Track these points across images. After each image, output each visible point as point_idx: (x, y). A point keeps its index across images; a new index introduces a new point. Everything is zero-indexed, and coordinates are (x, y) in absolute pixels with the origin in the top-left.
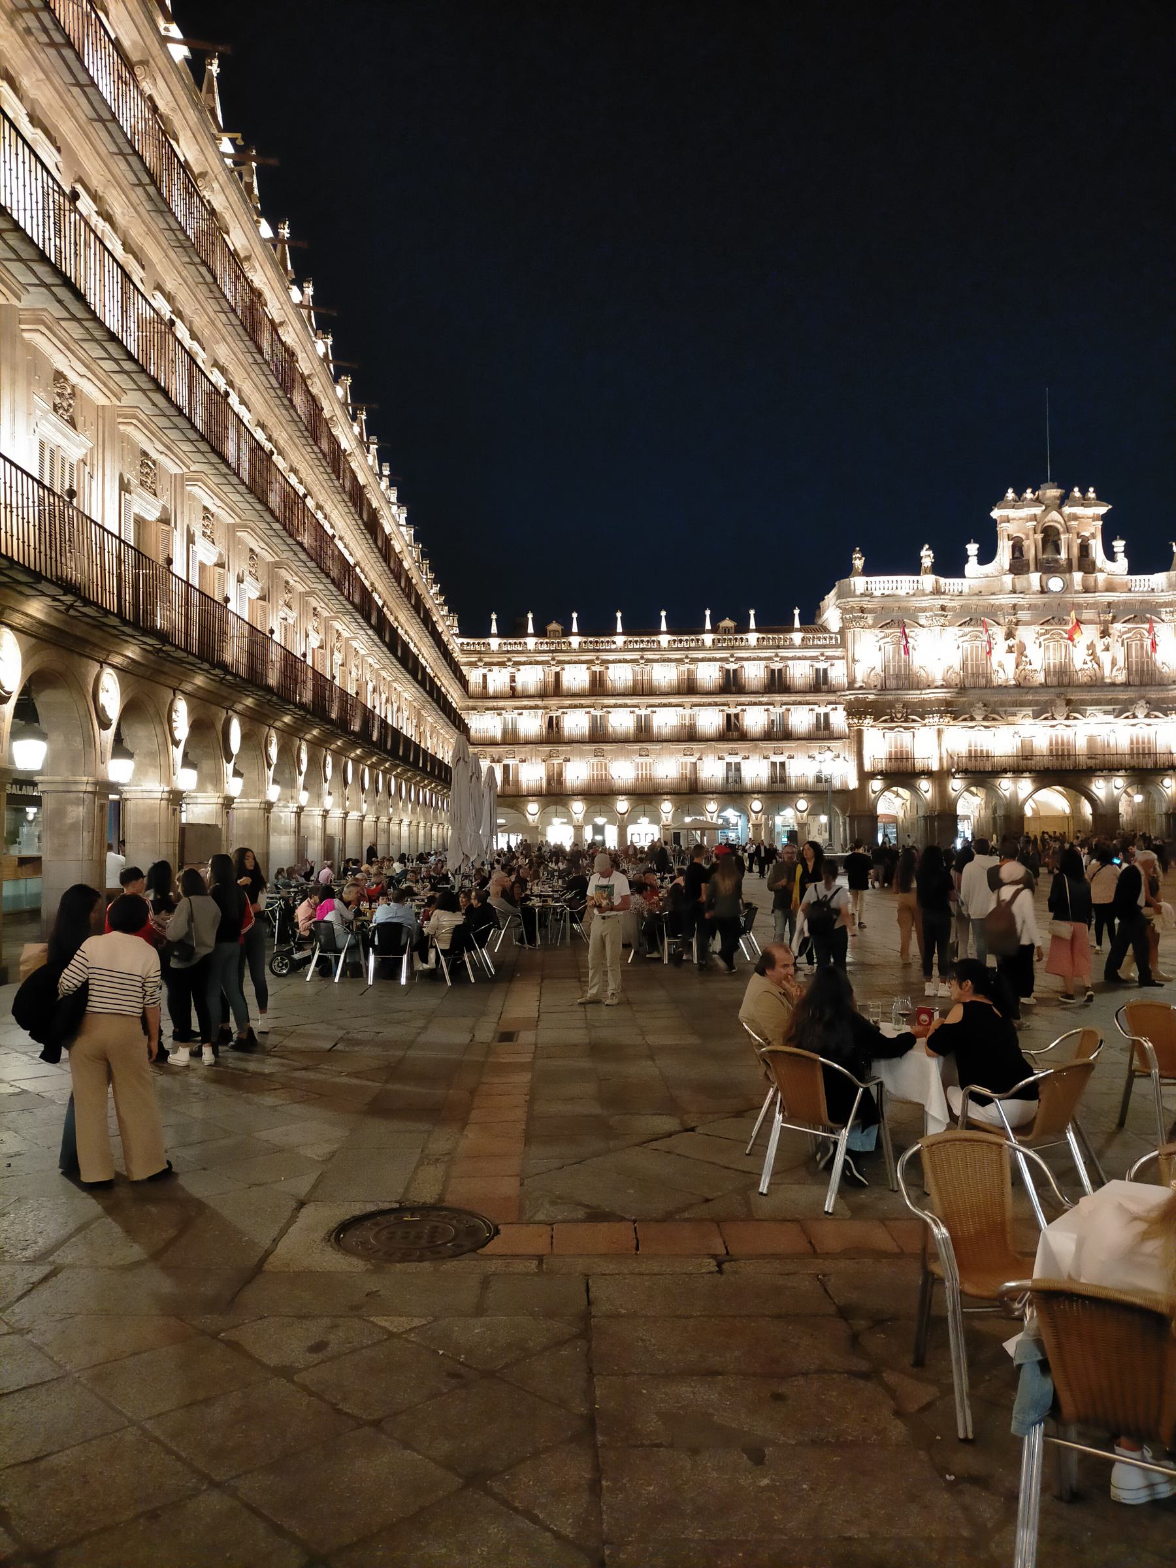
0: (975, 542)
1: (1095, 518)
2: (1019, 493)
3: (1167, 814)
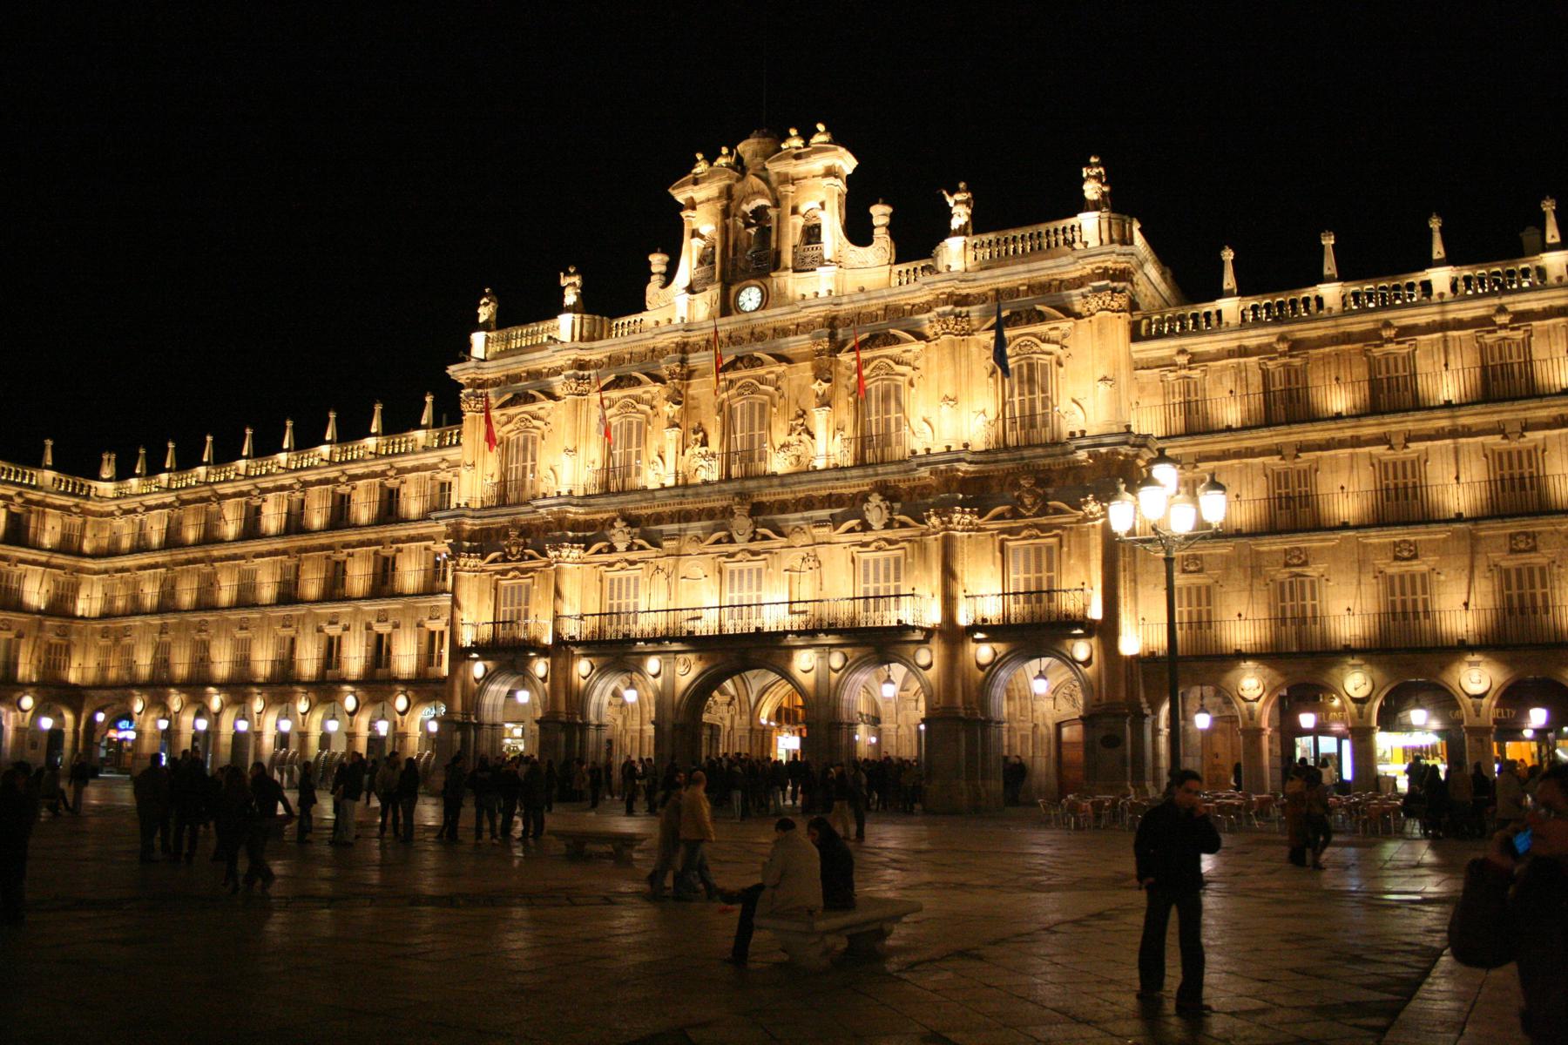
0: (663, 252)
1: (830, 172)
2: (711, 158)
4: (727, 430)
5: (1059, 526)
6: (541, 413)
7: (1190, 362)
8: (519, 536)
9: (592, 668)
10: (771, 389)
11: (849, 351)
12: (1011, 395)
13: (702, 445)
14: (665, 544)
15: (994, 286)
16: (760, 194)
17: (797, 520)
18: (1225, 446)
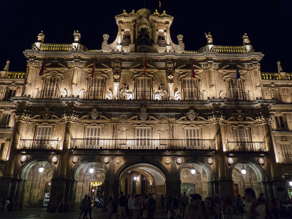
1: (167, 23)
2: (129, 11)
3: (211, 182)
4: (136, 86)
5: (249, 124)
6: (63, 71)
7: (275, 86)
8: (49, 110)
9: (79, 160)
10: (152, 76)
11: (180, 69)
12: (230, 87)
13: (127, 89)
14: (112, 118)
15: (223, 59)
16: (146, 24)
17: (163, 115)
18: (288, 108)
